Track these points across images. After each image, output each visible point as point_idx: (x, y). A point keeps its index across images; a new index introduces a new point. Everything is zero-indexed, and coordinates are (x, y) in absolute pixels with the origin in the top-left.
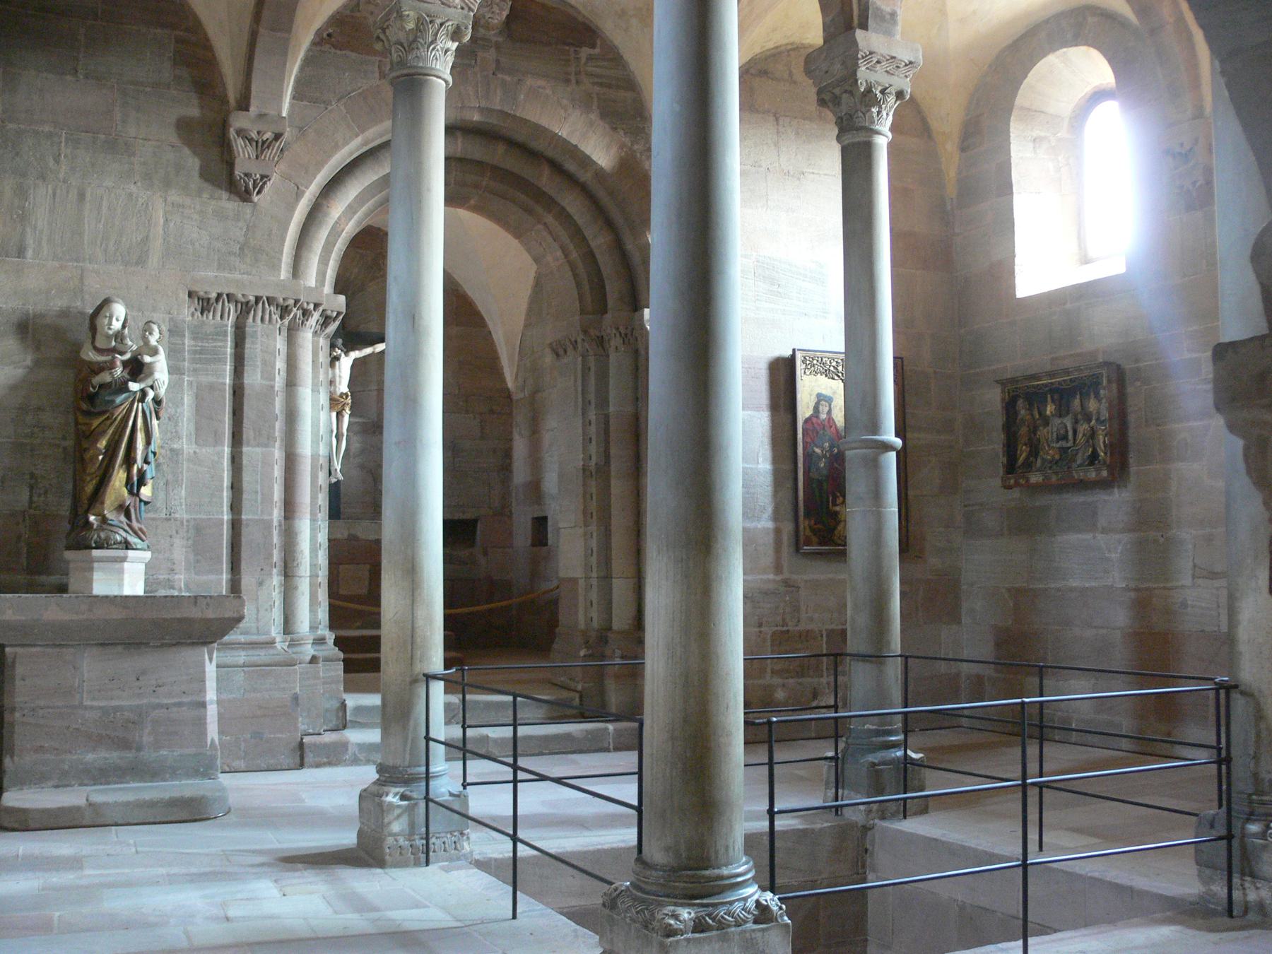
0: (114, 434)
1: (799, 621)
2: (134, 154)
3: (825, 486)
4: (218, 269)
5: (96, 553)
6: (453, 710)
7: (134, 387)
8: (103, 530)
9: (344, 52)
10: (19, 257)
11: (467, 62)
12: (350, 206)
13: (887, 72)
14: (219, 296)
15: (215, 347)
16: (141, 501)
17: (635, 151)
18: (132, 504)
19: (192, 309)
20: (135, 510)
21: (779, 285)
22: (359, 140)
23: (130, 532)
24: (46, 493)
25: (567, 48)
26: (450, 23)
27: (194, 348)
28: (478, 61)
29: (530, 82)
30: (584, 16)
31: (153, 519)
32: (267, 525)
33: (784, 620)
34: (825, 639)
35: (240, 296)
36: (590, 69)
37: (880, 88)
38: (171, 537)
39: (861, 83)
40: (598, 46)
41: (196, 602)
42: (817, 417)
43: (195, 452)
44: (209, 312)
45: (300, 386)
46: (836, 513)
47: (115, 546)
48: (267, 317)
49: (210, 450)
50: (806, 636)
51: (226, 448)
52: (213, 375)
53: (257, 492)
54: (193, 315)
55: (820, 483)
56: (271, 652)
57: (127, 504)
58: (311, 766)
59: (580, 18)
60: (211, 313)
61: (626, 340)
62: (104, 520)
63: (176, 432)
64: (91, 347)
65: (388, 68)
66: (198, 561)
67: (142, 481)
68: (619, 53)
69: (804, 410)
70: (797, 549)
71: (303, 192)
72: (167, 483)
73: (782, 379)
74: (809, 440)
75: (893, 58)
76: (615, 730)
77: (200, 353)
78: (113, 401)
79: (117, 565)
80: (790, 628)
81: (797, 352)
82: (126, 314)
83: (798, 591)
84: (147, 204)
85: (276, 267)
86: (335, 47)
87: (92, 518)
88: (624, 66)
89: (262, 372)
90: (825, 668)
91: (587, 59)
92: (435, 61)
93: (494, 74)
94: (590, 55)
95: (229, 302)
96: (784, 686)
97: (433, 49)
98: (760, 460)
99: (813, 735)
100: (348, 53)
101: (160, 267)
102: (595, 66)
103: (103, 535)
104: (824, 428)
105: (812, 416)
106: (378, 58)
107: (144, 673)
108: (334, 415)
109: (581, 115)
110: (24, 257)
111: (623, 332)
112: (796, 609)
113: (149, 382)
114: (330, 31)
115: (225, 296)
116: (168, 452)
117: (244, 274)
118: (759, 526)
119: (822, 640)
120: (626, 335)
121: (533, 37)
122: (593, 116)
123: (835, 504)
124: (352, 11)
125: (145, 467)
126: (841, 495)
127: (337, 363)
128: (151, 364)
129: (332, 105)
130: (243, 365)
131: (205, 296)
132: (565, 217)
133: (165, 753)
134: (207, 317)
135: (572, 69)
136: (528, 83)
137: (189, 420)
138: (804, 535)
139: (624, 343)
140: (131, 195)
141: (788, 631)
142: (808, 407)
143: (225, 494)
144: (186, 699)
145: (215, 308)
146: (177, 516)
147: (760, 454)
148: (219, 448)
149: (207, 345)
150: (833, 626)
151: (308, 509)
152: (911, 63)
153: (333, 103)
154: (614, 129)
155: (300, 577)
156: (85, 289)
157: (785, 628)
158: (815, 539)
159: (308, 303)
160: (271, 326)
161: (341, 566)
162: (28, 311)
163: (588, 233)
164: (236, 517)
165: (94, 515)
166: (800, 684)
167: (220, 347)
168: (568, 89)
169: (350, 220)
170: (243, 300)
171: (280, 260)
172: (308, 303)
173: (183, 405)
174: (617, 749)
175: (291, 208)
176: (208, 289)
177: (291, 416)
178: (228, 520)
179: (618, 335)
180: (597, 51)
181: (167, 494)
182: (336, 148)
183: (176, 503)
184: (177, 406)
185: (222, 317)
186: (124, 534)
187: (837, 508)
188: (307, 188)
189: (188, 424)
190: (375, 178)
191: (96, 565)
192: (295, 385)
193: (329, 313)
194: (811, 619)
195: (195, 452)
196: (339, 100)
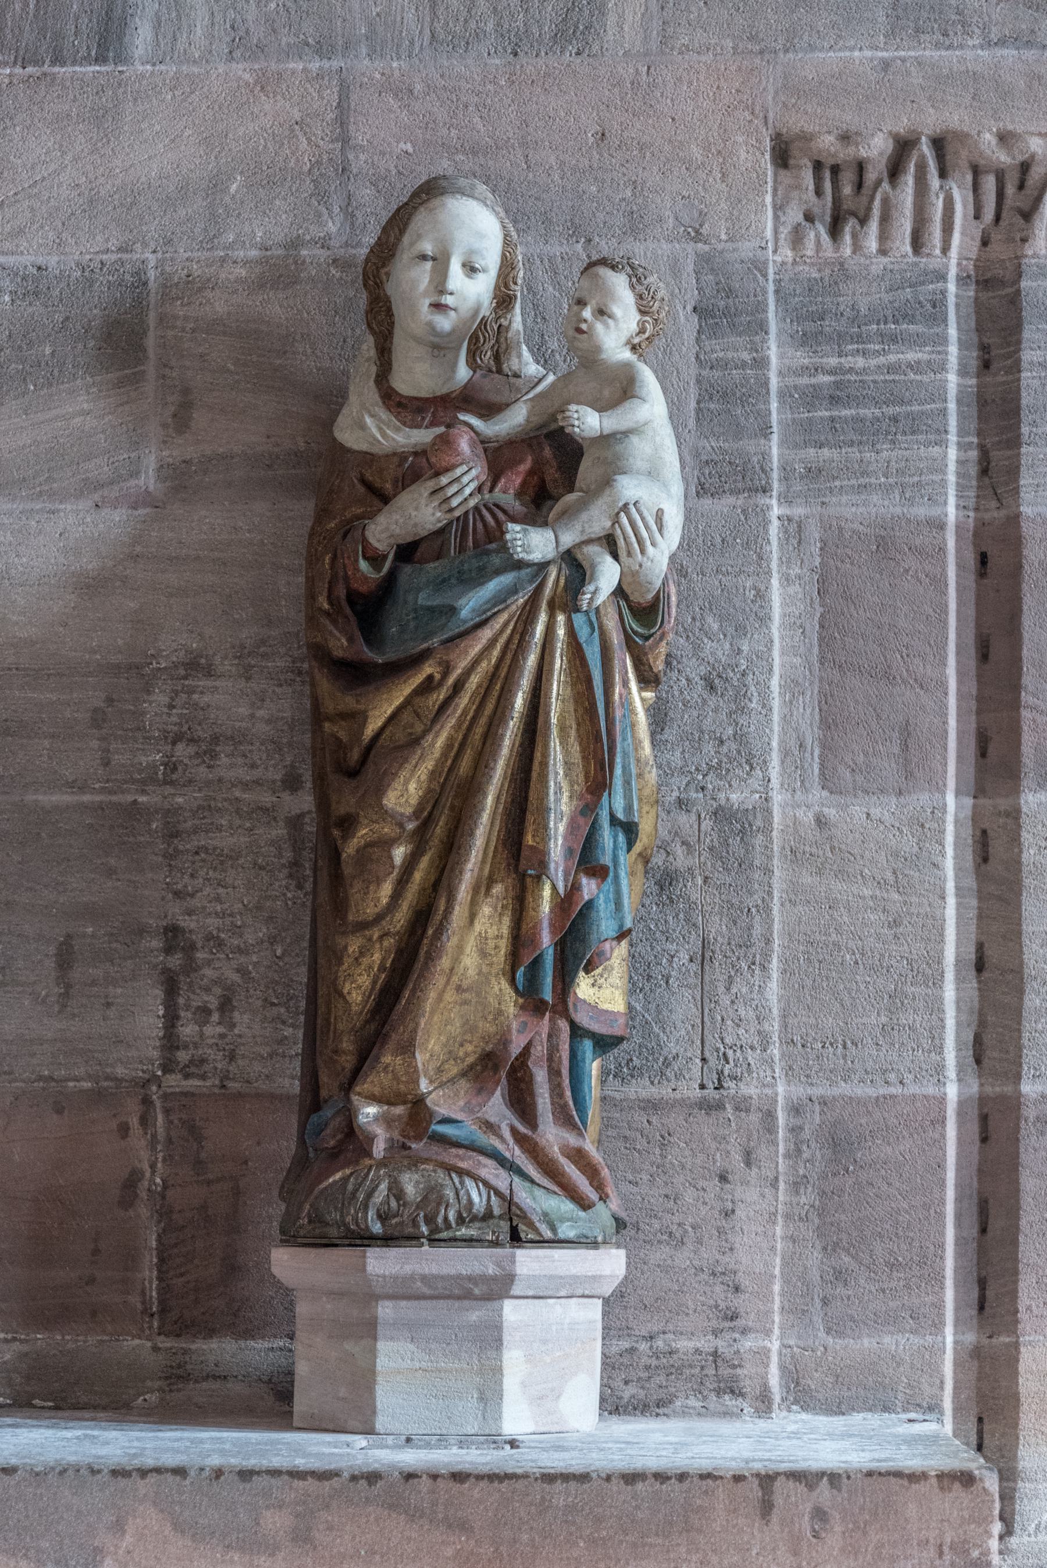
0: (455, 750)
4: (891, 34)
8: (415, 1162)
10: (102, 59)
14: (904, 146)
15: (891, 369)
16: (577, 1032)
18: (540, 1050)
19: (794, 215)
20: (554, 1073)
24: (226, 1005)
27: (805, 380)
31: (652, 1106)
35: (989, 138)
38: (723, 1178)
41: (766, 1507)
43: (821, 822)
44: (863, 221)
47: (463, 1232)
49: (884, 809)
51: (950, 799)
52: (888, 489)
54: (797, 238)
57: (515, 1050)
60: (874, 226)
63: (740, 737)
64: (371, 393)
66: (840, 1276)
72: (703, 958)
77: (834, 400)
78: (452, 611)
79: (475, 1315)
82: (507, 242)
87: (369, 1112)
95: (943, 174)
101: (654, 46)
103: (411, 1185)
110: (121, 58)
115: (925, 148)
116: (707, 824)
117: (1002, 42)
125: (589, 887)
128: (607, 440)
130: (1014, 442)
131: (844, 154)
134: (857, 247)
137: (792, 686)
143: (949, 993)
145: (886, 202)
146: (750, 1089)
148: (923, 799)
149: (860, 362)
156: (359, 161)
162: (139, 274)
164: (994, 1089)
165: (374, 1098)
167: (915, 367)
170: (1003, 158)
173: (765, 620)
176: (849, 119)
178: (961, 1104)
181: (705, 1000)
183: (747, 1036)
184: (741, 630)
185: (917, 242)
186: (501, 1179)
189: (789, 705)
191: (385, 1310)
195: (821, 822)
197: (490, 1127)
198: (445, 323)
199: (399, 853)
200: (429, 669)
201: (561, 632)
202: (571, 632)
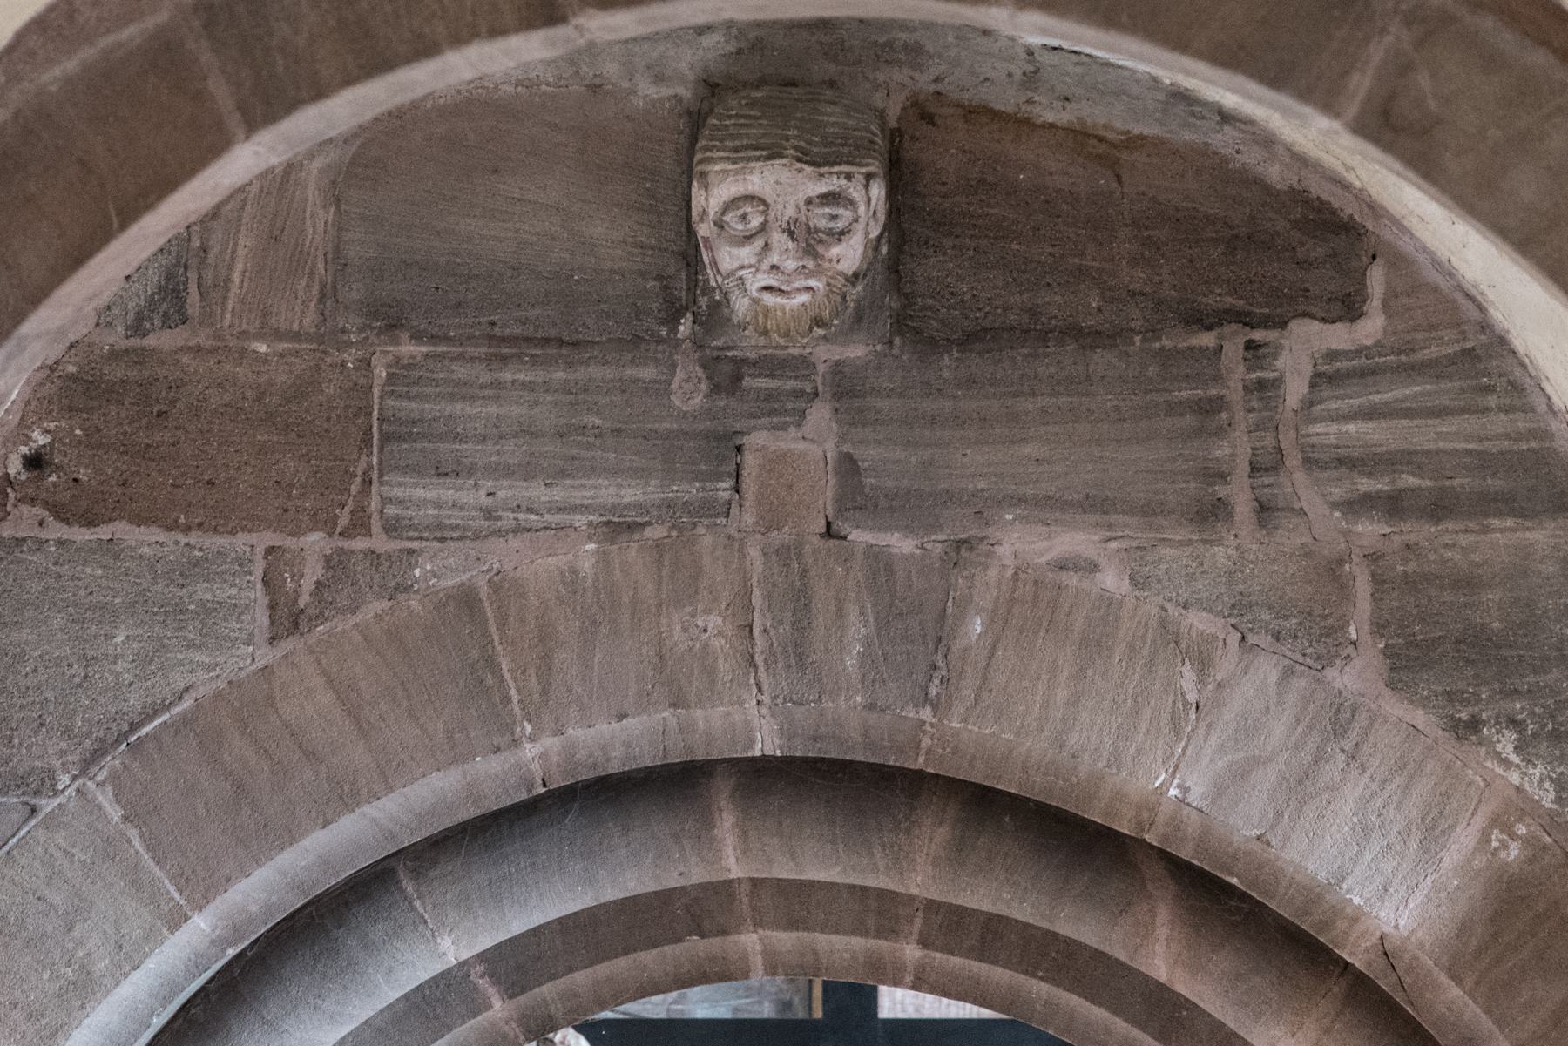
9: (103, 532)
11: (690, 491)
22: (201, 925)
25: (1207, 339)
30: (1301, 160)
36: (1325, 432)
40: (1374, 304)
59: (1275, 174)
65: (308, 585)
68: (1485, 326)
86: (61, 513)
88: (1516, 388)
91: (1317, 380)
93: (829, 533)
94: (1332, 355)
100: (120, 530)
109: (1288, 673)
114: (40, 439)
121: (1033, 313)
124: (137, 327)
129: (56, 793)
135: (1236, 449)
136: (1004, 551)
153: (65, 779)
154: (1464, 730)
168: (1221, 555)
180: (1371, 327)
196: (87, 765)
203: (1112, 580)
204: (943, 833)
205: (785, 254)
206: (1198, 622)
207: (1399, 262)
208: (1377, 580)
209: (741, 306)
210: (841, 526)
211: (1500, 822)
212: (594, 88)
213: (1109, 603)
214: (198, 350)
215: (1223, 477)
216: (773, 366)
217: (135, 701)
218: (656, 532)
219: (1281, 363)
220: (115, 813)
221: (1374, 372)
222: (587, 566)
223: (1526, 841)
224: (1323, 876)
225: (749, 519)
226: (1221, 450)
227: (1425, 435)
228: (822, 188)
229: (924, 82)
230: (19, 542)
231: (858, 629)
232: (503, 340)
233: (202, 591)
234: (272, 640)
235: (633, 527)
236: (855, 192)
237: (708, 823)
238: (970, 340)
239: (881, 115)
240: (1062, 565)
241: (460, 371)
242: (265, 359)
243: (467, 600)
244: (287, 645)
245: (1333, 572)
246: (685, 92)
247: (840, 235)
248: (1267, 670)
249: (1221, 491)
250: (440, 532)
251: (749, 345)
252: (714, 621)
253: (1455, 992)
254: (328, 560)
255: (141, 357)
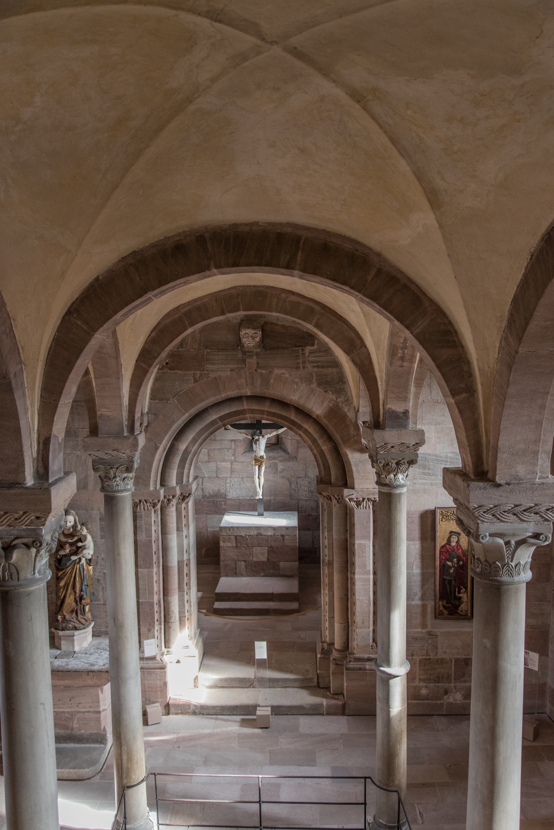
1: (437, 653)
2: (78, 436)
3: (453, 583)
5: (61, 633)
6: (251, 681)
7: (74, 558)
8: (64, 623)
9: (175, 371)
11: (240, 366)
12: (194, 438)
13: (400, 451)
17: (338, 403)
20: (81, 610)
21: (429, 469)
22: (187, 415)
23: (78, 622)
25: (297, 349)
26: (122, 466)
28: (247, 365)
29: (277, 371)
31: (98, 604)
32: (152, 605)
33: (427, 653)
34: (453, 663)
36: (310, 359)
37: (396, 461)
39: (380, 462)
41: (88, 675)
42: (450, 545)
45: (169, 534)
46: (460, 598)
48: (146, 508)
50: (441, 662)
53: (146, 589)
55: (450, 581)
56: (154, 662)
57: (75, 609)
58: (173, 714)
59: (305, 330)
61: (340, 501)
62: (64, 618)
65: (198, 377)
67: (81, 598)
68: (328, 347)
69: (440, 542)
70: (435, 618)
71: (159, 447)
72: (103, 588)
73: (429, 522)
74: (444, 558)
75: (402, 443)
76: (327, 705)
79: (71, 638)
80: (432, 657)
81: (437, 509)
83: (437, 638)
84: (86, 460)
85: (148, 485)
86: (170, 369)
87: (59, 617)
88: (331, 354)
89: (145, 534)
90: (453, 678)
91: (310, 353)
92: (117, 487)
93: (256, 370)
94: (311, 350)
96: (426, 687)
97: (115, 481)
98: (414, 568)
99: (445, 713)
100: (177, 371)
102: (313, 357)
103: (64, 625)
104: (453, 551)
105: (446, 544)
106: (194, 372)
107: (73, 698)
108: (257, 467)
109: (306, 385)
111: (337, 498)
112: (436, 648)
113: (80, 556)
118: (413, 603)
119: (452, 664)
120: (339, 499)
122: (314, 386)
123: (459, 592)
124: (178, 348)
126: (464, 588)
127: (258, 442)
132: (306, 432)
133: (83, 732)
135: (300, 361)
138: (439, 609)
139: (338, 502)
140: (78, 456)
141: (430, 659)
142: (444, 539)
144: (92, 710)
147: (414, 565)
150: (459, 656)
151: (177, 590)
152: (417, 444)
155: (172, 623)
157: (428, 657)
158: (446, 612)
159: (169, 496)
160: (149, 512)
161: (254, 549)
163: (320, 442)
166: (436, 686)
168: (299, 372)
169: (194, 445)
171: (149, 482)
172: (169, 496)
174: (328, 714)
175: (153, 455)
177: (165, 549)
179: (334, 498)
182: (174, 422)
187: (461, 595)
188: (160, 444)
190: (201, 427)
191: (62, 638)
192: (166, 534)
193: (184, 494)
194: (445, 652)
197: (73, 618)
198: (68, 528)
199: (62, 590)
200: (64, 571)
201: (78, 567)
202: (79, 567)
203: (287, 375)
204: (268, 404)
205: (250, 339)
206: (297, 380)
207: (319, 340)
208: (316, 375)
209: (245, 345)
210: (257, 370)
211: (330, 402)
212: (229, 321)
213: (287, 378)
214: (185, 351)
215: (299, 364)
216: (249, 352)
217: (179, 390)
218: (237, 371)
219: (306, 351)
220: (177, 402)
221: (316, 352)
222: (229, 374)
223: (333, 404)
224: (310, 408)
225: (247, 369)
226: (299, 361)
227: (321, 359)
228: (254, 332)
229: (266, 320)
230: (165, 372)
231: (259, 381)
232: (219, 349)
233: (186, 378)
234: (194, 383)
235: (234, 370)
236: (258, 332)
237: (243, 403)
238: (270, 349)
239: (261, 324)
240: (282, 374)
241: (214, 353)
242: (192, 352)
243: (216, 378)
244: (196, 384)
245: (311, 374)
246: (239, 321)
247: (256, 337)
248: (304, 385)
249: (299, 365)
250: (213, 371)
251: (246, 350)
252: (243, 380)
253: (325, 420)
254: (200, 374)
255: (179, 351)
